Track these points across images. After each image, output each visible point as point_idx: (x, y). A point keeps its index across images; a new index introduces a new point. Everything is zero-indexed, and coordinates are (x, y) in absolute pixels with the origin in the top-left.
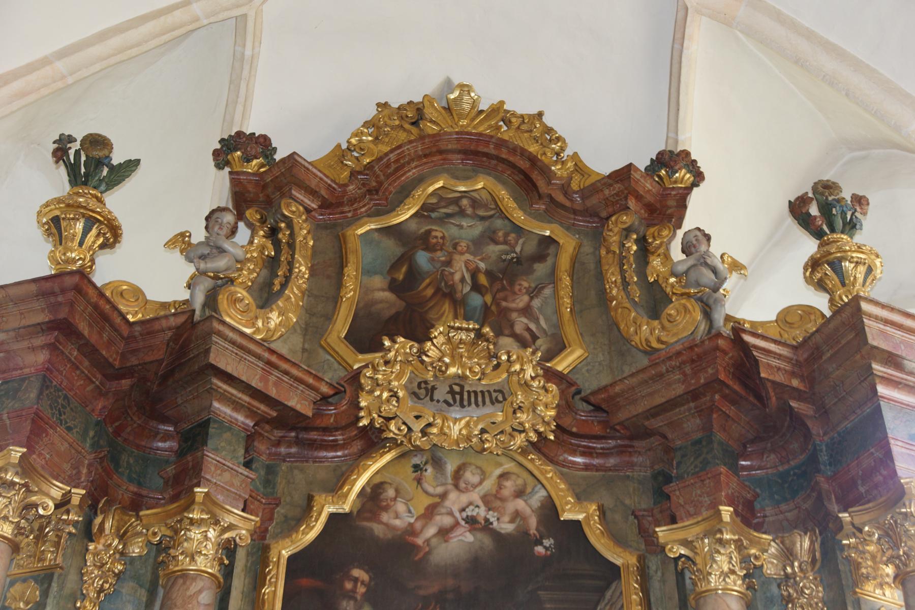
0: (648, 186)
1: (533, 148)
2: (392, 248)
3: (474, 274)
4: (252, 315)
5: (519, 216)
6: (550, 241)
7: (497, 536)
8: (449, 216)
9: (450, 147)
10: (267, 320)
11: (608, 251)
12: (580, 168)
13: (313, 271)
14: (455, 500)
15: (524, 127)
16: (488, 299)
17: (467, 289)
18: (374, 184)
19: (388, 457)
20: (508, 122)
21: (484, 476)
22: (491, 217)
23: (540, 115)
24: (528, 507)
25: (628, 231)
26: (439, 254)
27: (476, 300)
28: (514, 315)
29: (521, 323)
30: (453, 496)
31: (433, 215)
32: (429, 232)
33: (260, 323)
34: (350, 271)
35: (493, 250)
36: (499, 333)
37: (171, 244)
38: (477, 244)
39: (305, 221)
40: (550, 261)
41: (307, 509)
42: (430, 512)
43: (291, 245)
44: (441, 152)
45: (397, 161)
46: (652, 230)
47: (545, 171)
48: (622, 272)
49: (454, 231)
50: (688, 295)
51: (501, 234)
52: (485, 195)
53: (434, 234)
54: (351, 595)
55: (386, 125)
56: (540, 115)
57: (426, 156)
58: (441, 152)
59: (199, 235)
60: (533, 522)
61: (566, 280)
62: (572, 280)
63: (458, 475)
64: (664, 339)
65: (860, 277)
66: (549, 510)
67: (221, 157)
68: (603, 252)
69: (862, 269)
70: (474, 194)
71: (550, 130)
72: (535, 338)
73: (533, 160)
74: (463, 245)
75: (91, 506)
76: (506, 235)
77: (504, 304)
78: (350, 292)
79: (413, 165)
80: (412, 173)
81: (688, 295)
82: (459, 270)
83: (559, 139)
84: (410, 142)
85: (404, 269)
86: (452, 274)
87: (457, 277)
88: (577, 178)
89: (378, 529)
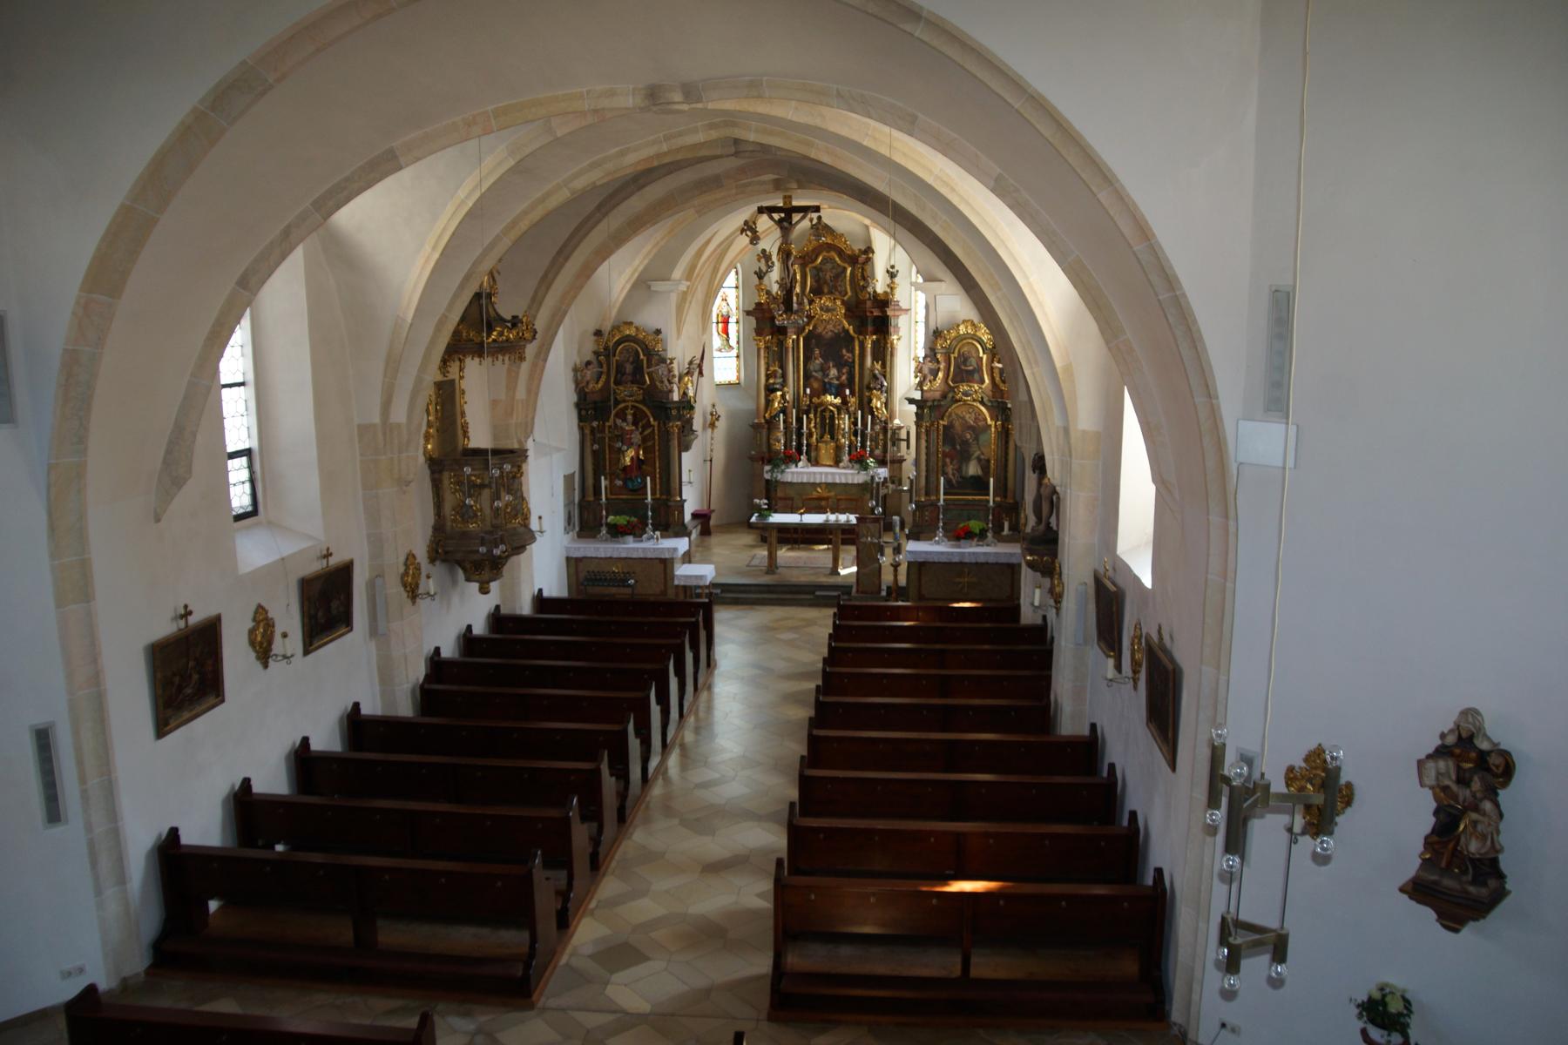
5: (839, 262)
14: (828, 327)
24: (840, 327)
29: (839, 288)
35: (834, 271)
42: (825, 328)
60: (841, 330)
66: (844, 327)
82: (828, 277)
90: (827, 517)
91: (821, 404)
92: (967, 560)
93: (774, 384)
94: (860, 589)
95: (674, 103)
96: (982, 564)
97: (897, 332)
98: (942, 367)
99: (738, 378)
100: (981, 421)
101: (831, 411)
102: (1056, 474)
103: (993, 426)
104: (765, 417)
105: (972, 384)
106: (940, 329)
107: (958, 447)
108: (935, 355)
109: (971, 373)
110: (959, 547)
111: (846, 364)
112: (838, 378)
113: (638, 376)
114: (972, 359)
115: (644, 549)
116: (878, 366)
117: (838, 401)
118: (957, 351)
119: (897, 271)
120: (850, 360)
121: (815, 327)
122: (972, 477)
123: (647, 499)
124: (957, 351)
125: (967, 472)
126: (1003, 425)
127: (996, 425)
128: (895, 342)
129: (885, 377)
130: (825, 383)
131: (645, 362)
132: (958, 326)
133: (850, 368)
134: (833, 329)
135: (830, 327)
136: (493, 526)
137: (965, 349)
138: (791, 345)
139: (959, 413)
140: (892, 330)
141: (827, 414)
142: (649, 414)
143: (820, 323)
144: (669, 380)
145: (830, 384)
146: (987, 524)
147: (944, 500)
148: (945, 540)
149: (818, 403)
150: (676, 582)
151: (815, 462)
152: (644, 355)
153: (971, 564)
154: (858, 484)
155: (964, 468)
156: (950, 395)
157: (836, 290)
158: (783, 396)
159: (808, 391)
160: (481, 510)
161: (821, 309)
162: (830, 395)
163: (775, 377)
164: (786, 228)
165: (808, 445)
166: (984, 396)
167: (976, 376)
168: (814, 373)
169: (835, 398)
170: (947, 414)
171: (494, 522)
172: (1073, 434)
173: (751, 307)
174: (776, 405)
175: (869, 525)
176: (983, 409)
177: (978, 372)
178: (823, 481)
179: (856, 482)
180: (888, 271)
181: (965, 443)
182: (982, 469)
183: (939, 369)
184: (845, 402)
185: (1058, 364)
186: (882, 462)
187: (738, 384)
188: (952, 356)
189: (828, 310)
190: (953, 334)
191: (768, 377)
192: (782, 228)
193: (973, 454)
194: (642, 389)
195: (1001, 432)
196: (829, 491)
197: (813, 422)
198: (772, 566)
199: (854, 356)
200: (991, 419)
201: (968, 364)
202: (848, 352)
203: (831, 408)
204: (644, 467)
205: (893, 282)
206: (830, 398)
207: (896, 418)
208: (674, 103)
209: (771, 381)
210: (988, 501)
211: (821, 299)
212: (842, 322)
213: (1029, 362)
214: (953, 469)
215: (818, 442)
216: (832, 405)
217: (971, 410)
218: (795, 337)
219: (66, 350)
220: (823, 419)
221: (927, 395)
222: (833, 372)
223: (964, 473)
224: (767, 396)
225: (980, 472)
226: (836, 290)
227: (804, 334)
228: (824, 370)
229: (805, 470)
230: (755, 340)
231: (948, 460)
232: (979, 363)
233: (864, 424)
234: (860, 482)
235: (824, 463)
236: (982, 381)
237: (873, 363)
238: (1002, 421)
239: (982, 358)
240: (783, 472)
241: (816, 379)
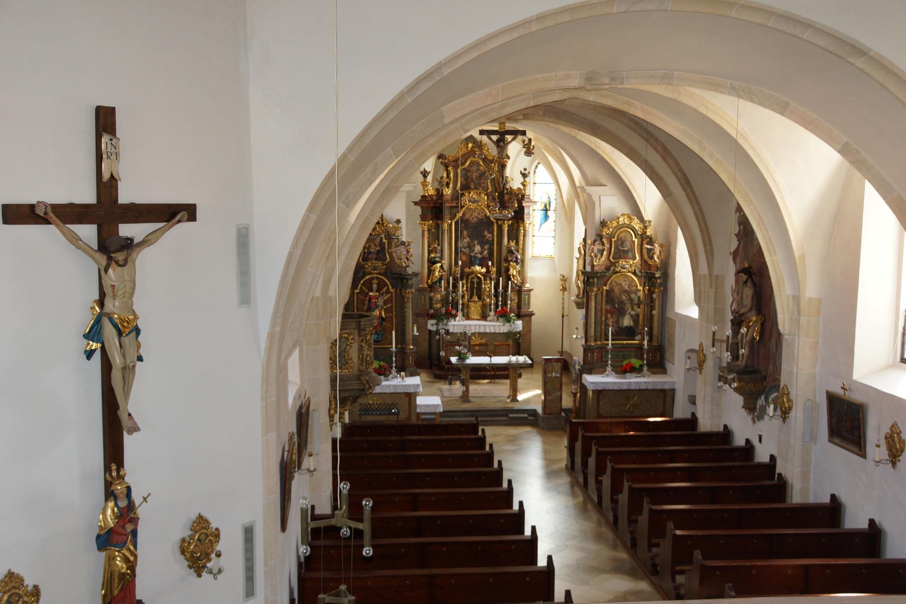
3: (476, 176)
7: (479, 219)
14: (474, 214)
27: (476, 181)
29: (483, 185)
35: (479, 172)
36: (480, 187)
38: (477, 171)
41: (455, 216)
42: (471, 216)
66: (486, 214)
74: (474, 171)
82: (474, 176)
89: (464, 218)
90: (510, 359)
91: (472, 273)
92: (633, 388)
93: (435, 257)
94: (546, 412)
95: (605, 84)
96: (644, 390)
97: (529, 218)
98: (606, 248)
100: (633, 286)
101: (479, 278)
102: (787, 327)
103: (642, 290)
104: (427, 283)
105: (627, 260)
106: (605, 221)
107: (617, 306)
108: (601, 239)
109: (626, 252)
110: (625, 378)
111: (487, 242)
112: (481, 253)
113: (381, 255)
114: (627, 242)
115: (394, 386)
116: (513, 244)
117: (484, 270)
118: (616, 237)
119: (529, 173)
121: (464, 214)
122: (626, 327)
123: (392, 348)
124: (616, 237)
125: (622, 324)
126: (649, 290)
127: (644, 290)
128: (527, 225)
129: (518, 251)
130: (471, 257)
131: (386, 244)
132: (618, 218)
133: (490, 245)
134: (477, 215)
135: (475, 214)
136: (359, 371)
137: (623, 235)
139: (618, 281)
140: (525, 217)
141: (475, 280)
142: (389, 283)
143: (468, 210)
144: (407, 258)
145: (475, 257)
146: (643, 361)
147: (612, 344)
148: (614, 373)
149: (470, 272)
150: (418, 410)
151: (467, 317)
152: (386, 239)
153: (636, 390)
154: (504, 333)
155: (621, 320)
156: (612, 268)
157: (480, 186)
158: (441, 267)
160: (351, 359)
161: (470, 201)
162: (479, 266)
163: (436, 252)
164: (501, 147)
165: (463, 304)
166: (636, 268)
167: (630, 255)
169: (482, 268)
170: (609, 282)
171: (361, 368)
172: (803, 302)
173: (418, 199)
174: (437, 273)
175: (553, 364)
176: (636, 279)
177: (631, 251)
178: (477, 331)
179: (502, 331)
180: (521, 173)
181: (622, 303)
182: (634, 322)
183: (603, 250)
184: (488, 271)
185: (797, 253)
186: (519, 316)
188: (613, 240)
189: (474, 202)
190: (615, 224)
191: (430, 252)
192: (498, 146)
193: (627, 311)
194: (385, 265)
195: (648, 294)
196: (481, 339)
197: (465, 286)
198: (465, 397)
199: (493, 236)
200: (640, 285)
201: (624, 245)
202: (489, 233)
203: (479, 275)
204: (384, 323)
205: (525, 181)
206: (478, 268)
207: (527, 283)
208: (605, 84)
209: (433, 255)
210: (608, 345)
211: (470, 193)
212: (485, 211)
213: (770, 253)
214: (612, 322)
215: (469, 301)
216: (480, 273)
217: (626, 279)
218: (450, 222)
219: (290, 252)
220: (472, 283)
221: (596, 269)
222: (478, 248)
223: (620, 325)
224: (429, 267)
225: (632, 324)
226: (480, 186)
227: (455, 220)
228: (470, 247)
229: (461, 323)
230: (422, 224)
231: (609, 315)
232: (632, 245)
233: (505, 288)
234: (505, 331)
235: (472, 317)
236: (634, 258)
237: (508, 241)
238: (648, 286)
239: (634, 241)
240: (446, 324)
241: (464, 253)
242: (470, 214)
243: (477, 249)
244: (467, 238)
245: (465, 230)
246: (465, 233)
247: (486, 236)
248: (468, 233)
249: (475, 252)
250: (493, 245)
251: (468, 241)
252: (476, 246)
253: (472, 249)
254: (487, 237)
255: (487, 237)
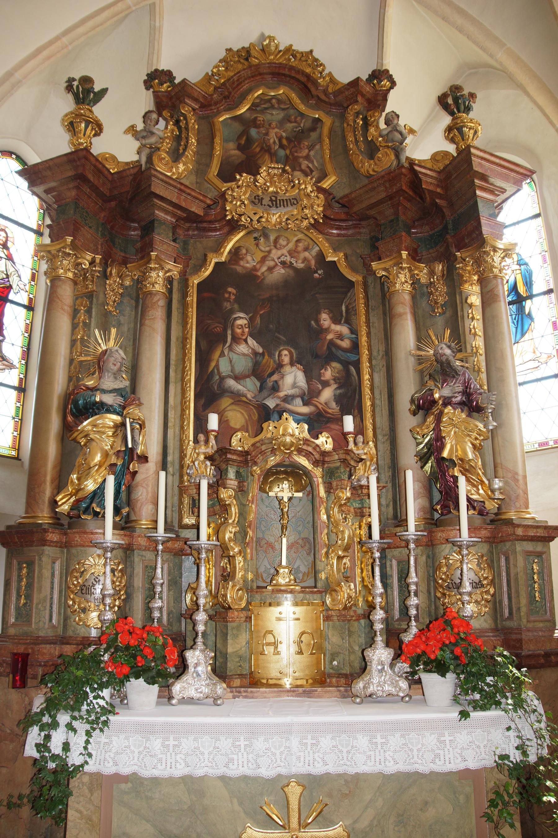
0: (368, 89)
1: (308, 70)
2: (237, 127)
3: (280, 139)
4: (170, 166)
5: (302, 108)
6: (318, 120)
7: (296, 270)
8: (266, 109)
9: (265, 71)
10: (177, 168)
11: (348, 125)
12: (333, 80)
13: (198, 141)
14: (275, 254)
15: (303, 59)
16: (288, 152)
17: (277, 147)
18: (227, 93)
19: (241, 234)
20: (294, 56)
21: (289, 241)
22: (288, 108)
23: (311, 51)
24: (310, 255)
25: (358, 114)
26: (262, 129)
27: (282, 153)
28: (301, 160)
29: (304, 164)
30: (274, 251)
31: (258, 109)
32: (256, 118)
33: (174, 170)
34: (217, 140)
35: (289, 126)
36: (293, 169)
37: (127, 132)
38: (281, 124)
39: (193, 115)
40: (318, 131)
41: (204, 262)
42: (263, 260)
43: (187, 129)
44: (260, 74)
45: (238, 80)
46: (370, 113)
47: (315, 83)
48: (355, 136)
49: (269, 117)
50: (388, 147)
51: (293, 117)
52: (284, 97)
53: (259, 119)
54: (228, 300)
55: (231, 61)
56: (311, 51)
57: (253, 77)
58: (260, 74)
59: (140, 126)
60: (313, 262)
61: (327, 141)
62: (330, 140)
63: (276, 241)
64: (376, 170)
65: (471, 136)
66: (321, 256)
67: (148, 84)
68: (345, 125)
69: (472, 132)
70: (279, 97)
71: (316, 60)
72: (312, 171)
73: (308, 76)
75: (105, 263)
76: (296, 118)
77: (296, 154)
78: (218, 152)
79: (246, 82)
80: (246, 87)
81: (388, 147)
82: (272, 137)
83: (321, 65)
84: (244, 69)
85: (244, 138)
86: (269, 140)
87: (272, 141)
88: (331, 86)
89: (239, 269)
99: (17, 445)
104: (54, 504)
120: (346, 344)
121: (236, 253)
133: (346, 364)
134: (288, 259)
138: (159, 288)
143: (250, 243)
159: (213, 422)
161: (257, 200)
168: (231, 383)
187: (17, 458)
202: (336, 320)
242: (259, 256)
243: (289, 380)
244: (250, 340)
245: (241, 310)
246: (239, 322)
247: (328, 330)
248: (251, 320)
249: (282, 394)
250: (357, 364)
251: (255, 353)
252: (287, 369)
253: (270, 383)
254: (330, 337)
255: (330, 337)
